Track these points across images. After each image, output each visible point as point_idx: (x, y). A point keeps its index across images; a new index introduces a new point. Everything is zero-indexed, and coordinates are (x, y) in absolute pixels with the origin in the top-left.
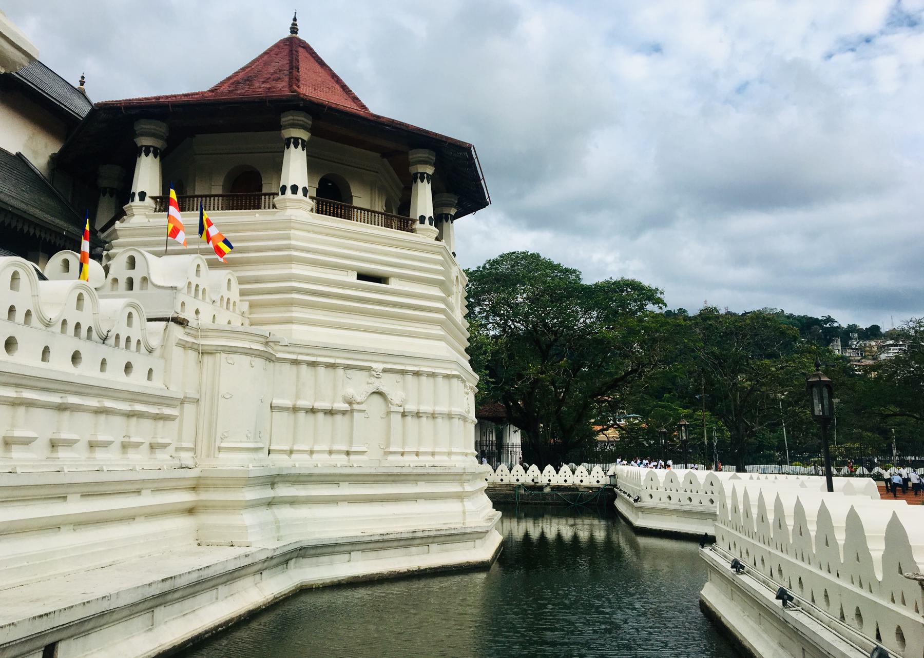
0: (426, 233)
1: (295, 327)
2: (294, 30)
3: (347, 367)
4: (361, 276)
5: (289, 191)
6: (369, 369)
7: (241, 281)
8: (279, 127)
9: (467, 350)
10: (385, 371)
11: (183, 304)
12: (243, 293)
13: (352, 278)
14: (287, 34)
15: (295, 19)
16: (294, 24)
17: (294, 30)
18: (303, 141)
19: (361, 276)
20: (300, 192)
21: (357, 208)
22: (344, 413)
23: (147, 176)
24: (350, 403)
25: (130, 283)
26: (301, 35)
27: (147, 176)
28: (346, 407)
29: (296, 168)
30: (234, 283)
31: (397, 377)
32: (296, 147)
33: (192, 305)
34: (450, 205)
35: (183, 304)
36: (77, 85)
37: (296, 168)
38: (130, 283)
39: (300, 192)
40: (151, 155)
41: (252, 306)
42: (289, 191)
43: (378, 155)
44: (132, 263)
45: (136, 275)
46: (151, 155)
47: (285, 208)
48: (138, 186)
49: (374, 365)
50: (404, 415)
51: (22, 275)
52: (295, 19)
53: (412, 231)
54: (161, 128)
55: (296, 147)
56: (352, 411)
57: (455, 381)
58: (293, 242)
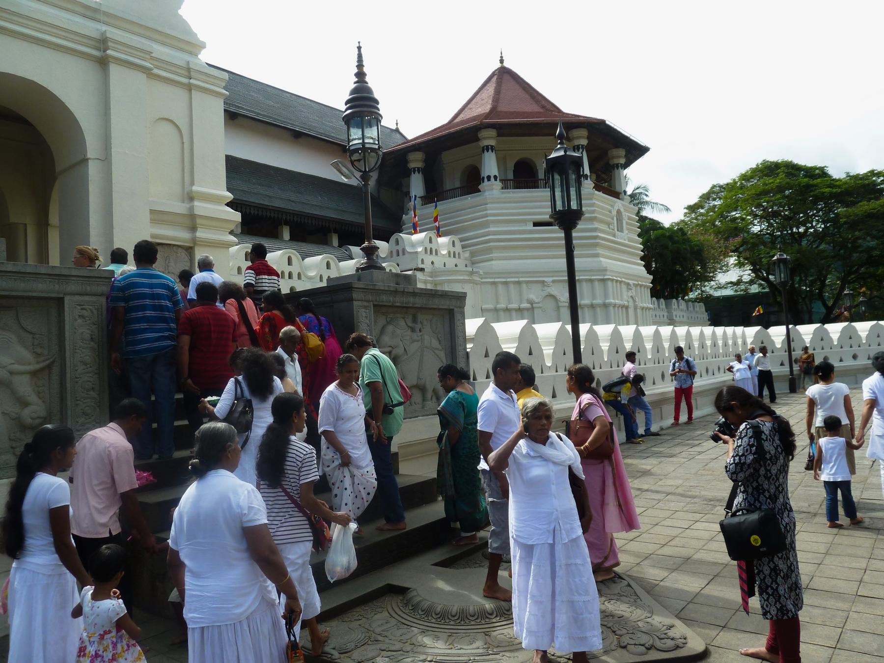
1: (493, 262)
2: (502, 61)
3: (527, 282)
4: (536, 224)
5: (486, 180)
6: (543, 282)
7: (461, 240)
8: (478, 139)
9: (642, 259)
10: (554, 281)
11: (422, 260)
12: (463, 247)
13: (530, 227)
14: (499, 65)
16: (502, 57)
17: (502, 61)
18: (492, 146)
19: (536, 224)
20: (492, 179)
22: (528, 309)
23: (417, 186)
24: (532, 304)
25: (398, 252)
26: (506, 64)
27: (417, 186)
28: (529, 306)
30: (458, 243)
33: (428, 259)
34: (619, 157)
35: (422, 260)
36: (394, 127)
38: (398, 252)
39: (492, 179)
41: (473, 254)
44: (397, 243)
45: (400, 248)
47: (484, 191)
48: (413, 194)
49: (546, 279)
51: (331, 261)
54: (419, 155)
56: (533, 308)
57: (609, 283)
58: (489, 212)
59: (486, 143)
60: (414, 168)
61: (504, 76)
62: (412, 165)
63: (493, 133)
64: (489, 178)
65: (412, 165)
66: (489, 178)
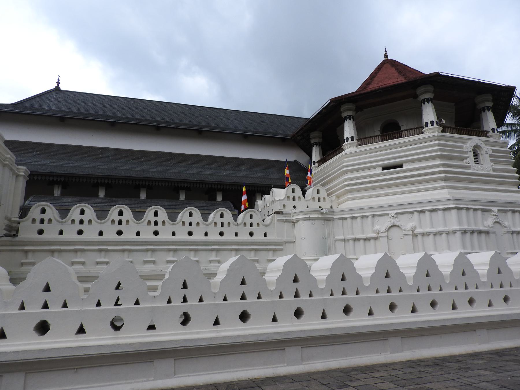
2: (386, 56)
14: (383, 59)
15: (386, 51)
17: (386, 56)
20: (435, 124)
26: (390, 57)
29: (429, 114)
31: (504, 214)
32: (428, 103)
37: (429, 114)
40: (352, 120)
42: (429, 125)
46: (352, 120)
50: (513, 233)
52: (386, 51)
53: (487, 137)
55: (428, 103)
59: (422, 97)
62: (344, 115)
63: (431, 88)
64: (427, 124)
66: (427, 124)
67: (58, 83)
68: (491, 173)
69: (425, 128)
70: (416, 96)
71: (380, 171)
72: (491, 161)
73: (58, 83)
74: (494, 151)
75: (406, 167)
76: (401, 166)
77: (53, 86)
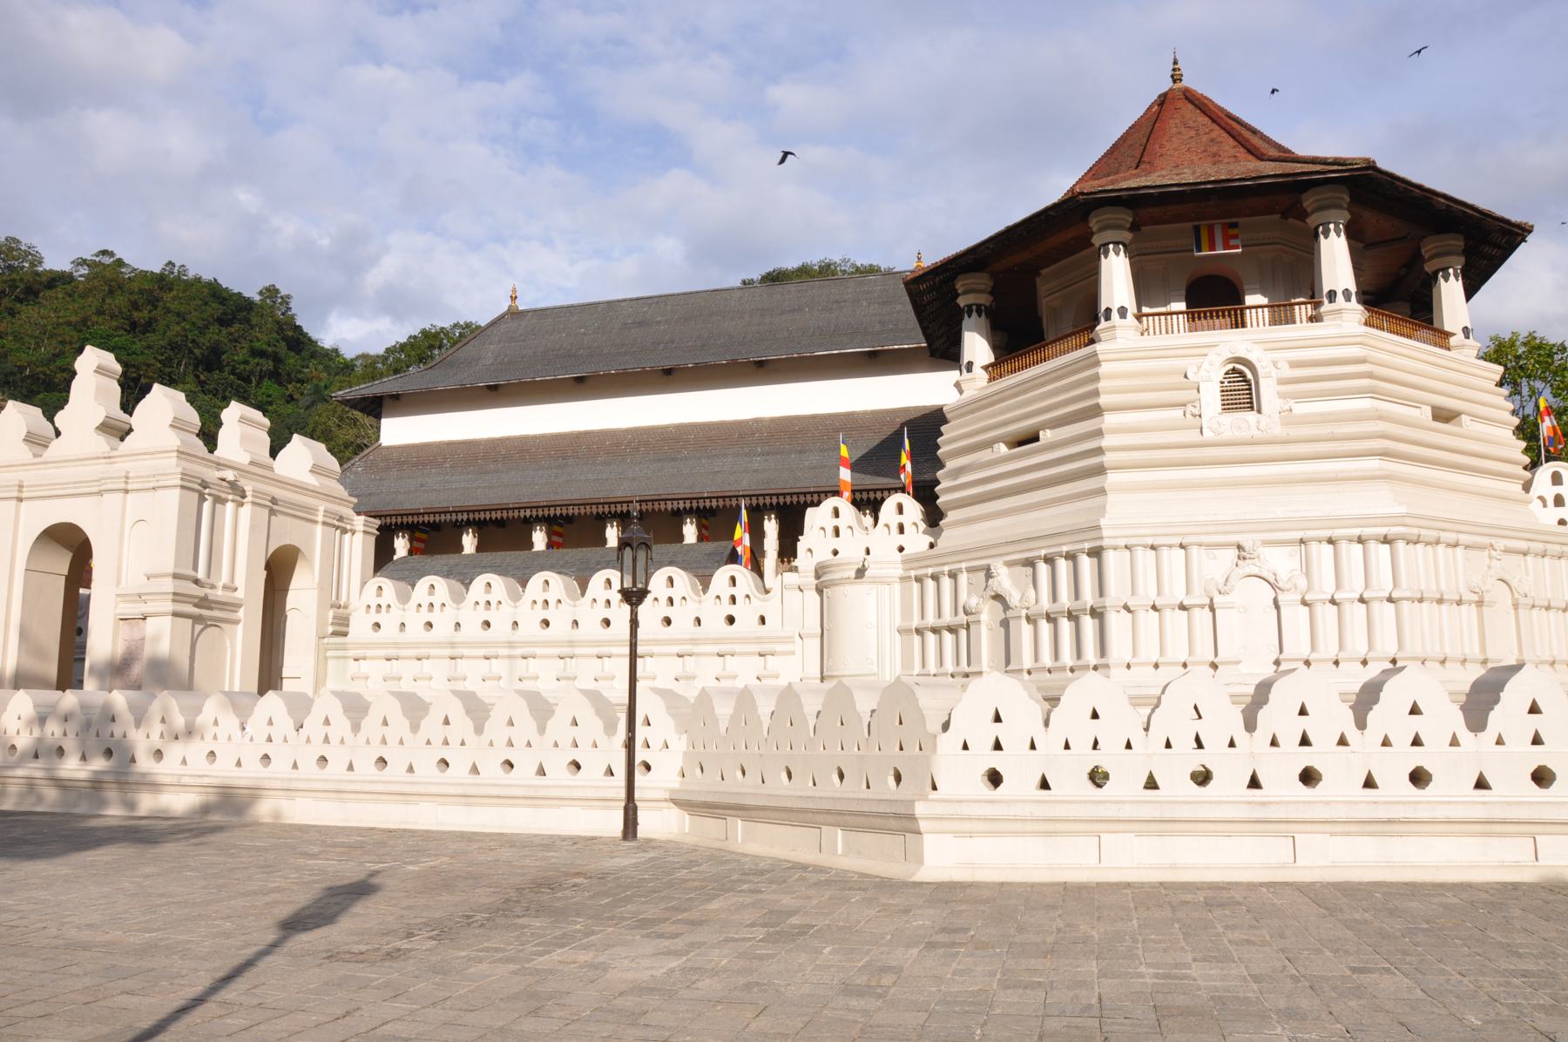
0: (1348, 318)
14: (1166, 85)
15: (1175, 63)
17: (1176, 78)
21: (1250, 308)
26: (1187, 82)
40: (974, 314)
43: (1277, 217)
46: (974, 314)
52: (1175, 63)
54: (982, 280)
60: (969, 307)
61: (1178, 105)
65: (962, 302)
67: (514, 298)
68: (1278, 431)
69: (1103, 324)
70: (1084, 241)
71: (1002, 449)
72: (1282, 395)
73: (514, 298)
74: (1295, 365)
75: (1046, 436)
76: (1036, 439)
77: (504, 307)
